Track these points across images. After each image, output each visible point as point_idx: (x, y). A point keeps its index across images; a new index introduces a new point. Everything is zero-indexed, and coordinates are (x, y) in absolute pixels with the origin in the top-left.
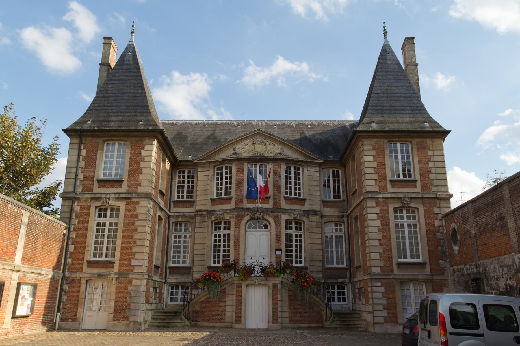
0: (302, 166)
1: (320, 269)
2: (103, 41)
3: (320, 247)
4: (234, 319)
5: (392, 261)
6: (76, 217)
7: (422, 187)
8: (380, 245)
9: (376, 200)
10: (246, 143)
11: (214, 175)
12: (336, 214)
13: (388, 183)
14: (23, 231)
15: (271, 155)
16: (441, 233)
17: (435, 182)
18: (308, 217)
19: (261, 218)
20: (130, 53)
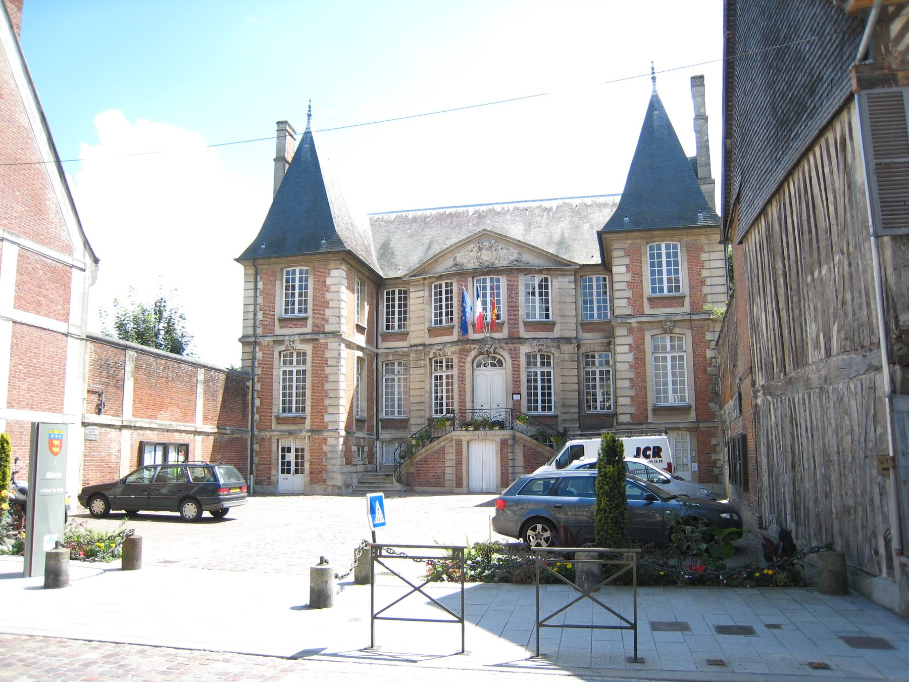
0: (551, 275)
1: (576, 416)
2: (276, 127)
3: (576, 387)
4: (454, 483)
5: (647, 406)
6: (259, 365)
7: (692, 304)
8: (632, 387)
9: (629, 326)
10: (470, 250)
11: (430, 296)
12: (599, 341)
13: (646, 302)
14: (200, 389)
15: (504, 263)
16: (713, 367)
17: (709, 297)
18: (559, 347)
19: (492, 352)
20: (307, 146)
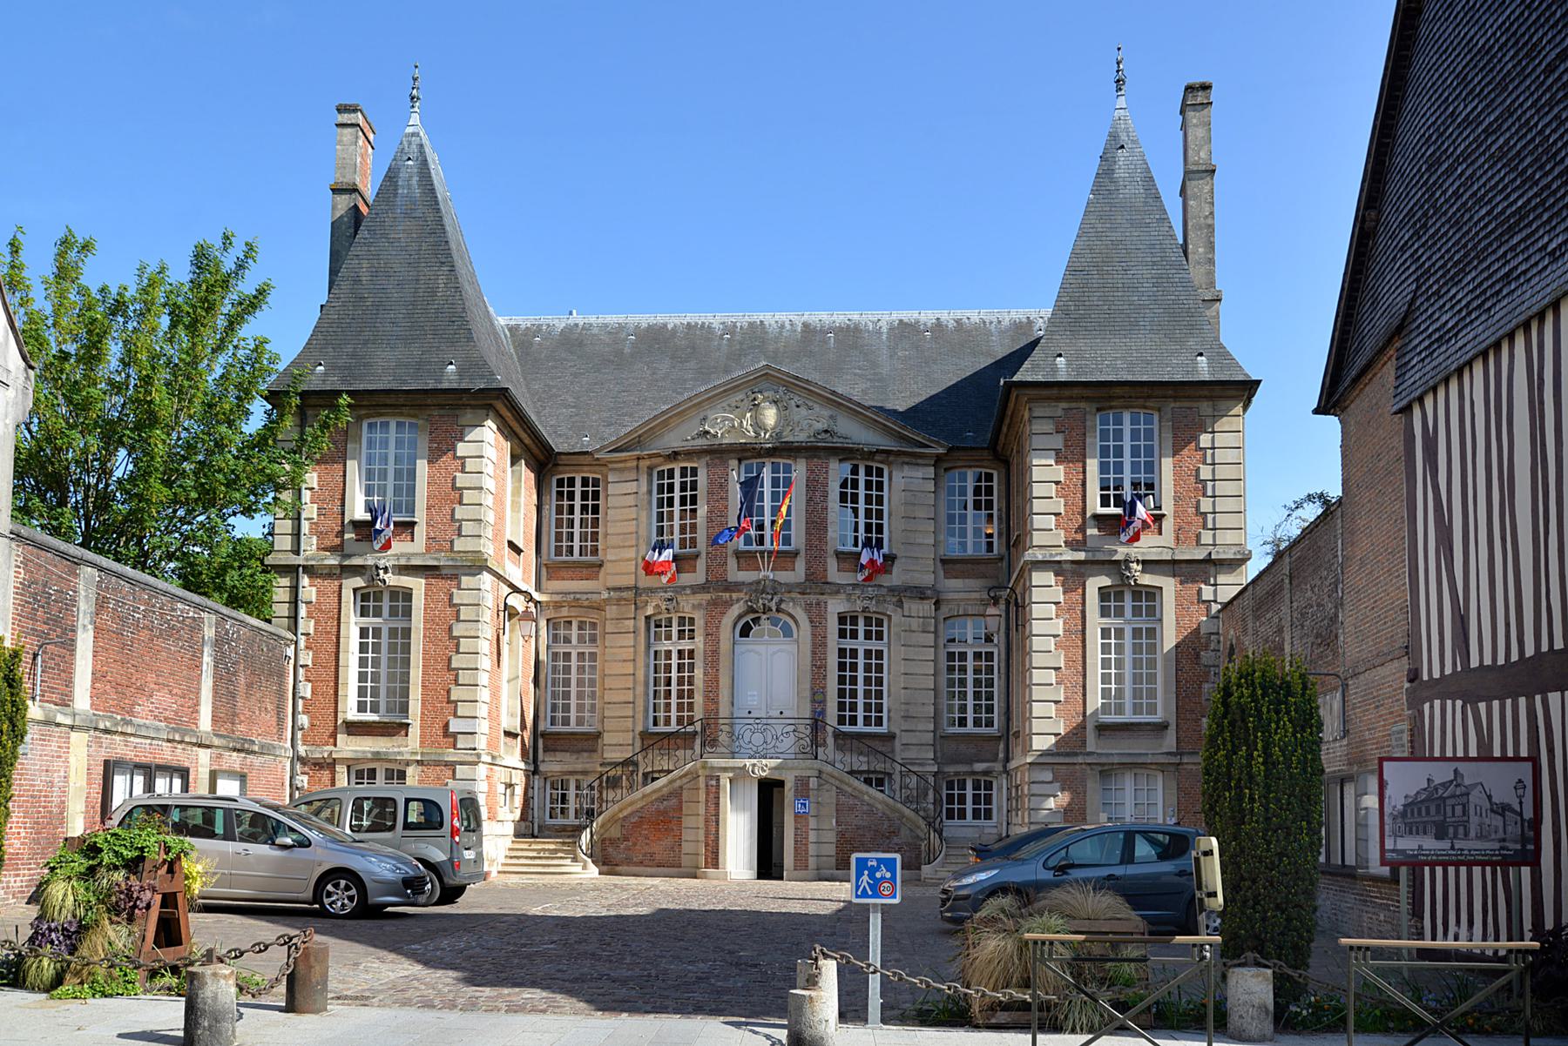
0: (889, 464)
1: (929, 737)
6: (310, 616)
10: (733, 405)
14: (207, 659)
18: (900, 604)
19: (774, 609)
